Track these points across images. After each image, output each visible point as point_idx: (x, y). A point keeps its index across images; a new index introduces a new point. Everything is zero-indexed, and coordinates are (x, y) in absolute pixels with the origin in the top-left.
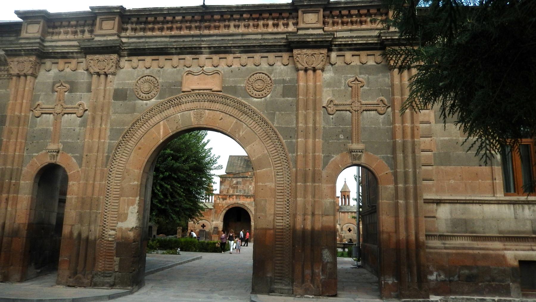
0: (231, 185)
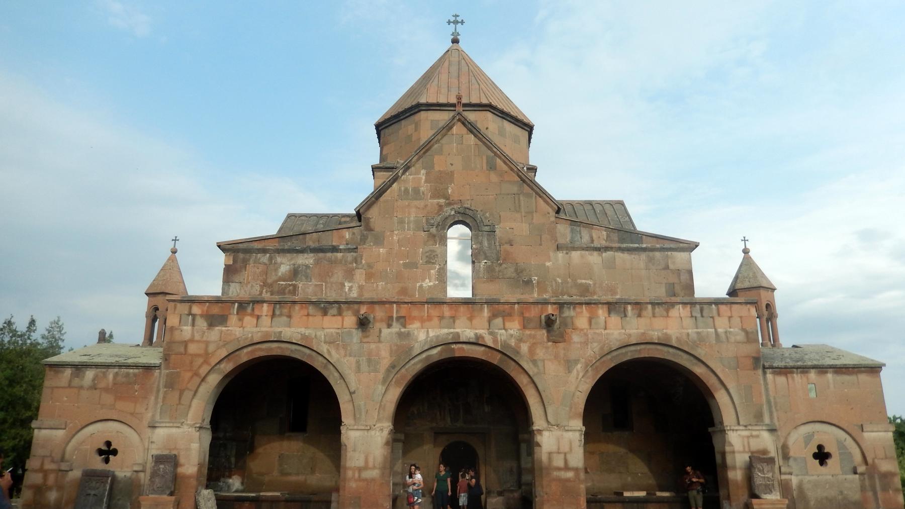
0: (269, 281)
